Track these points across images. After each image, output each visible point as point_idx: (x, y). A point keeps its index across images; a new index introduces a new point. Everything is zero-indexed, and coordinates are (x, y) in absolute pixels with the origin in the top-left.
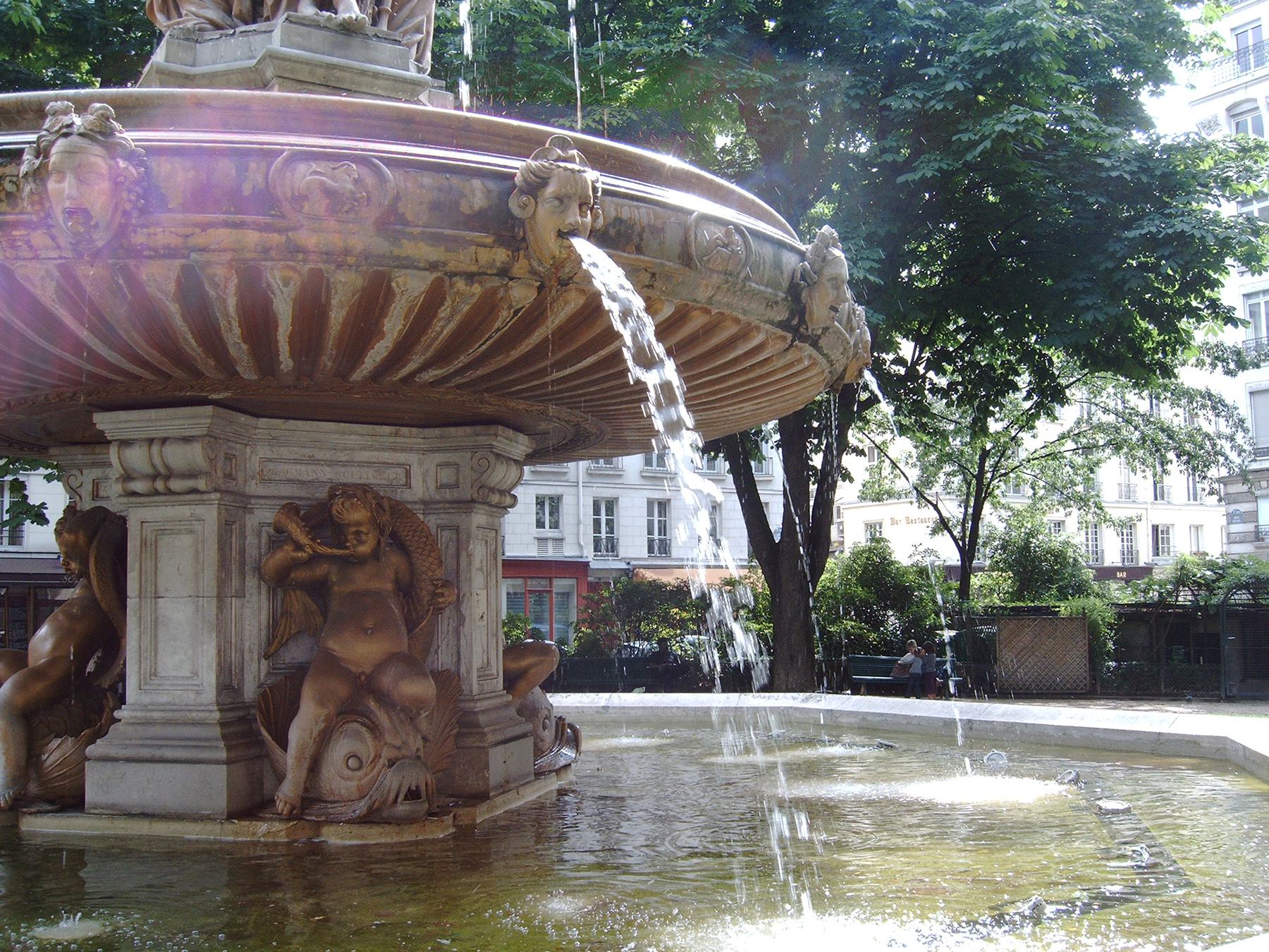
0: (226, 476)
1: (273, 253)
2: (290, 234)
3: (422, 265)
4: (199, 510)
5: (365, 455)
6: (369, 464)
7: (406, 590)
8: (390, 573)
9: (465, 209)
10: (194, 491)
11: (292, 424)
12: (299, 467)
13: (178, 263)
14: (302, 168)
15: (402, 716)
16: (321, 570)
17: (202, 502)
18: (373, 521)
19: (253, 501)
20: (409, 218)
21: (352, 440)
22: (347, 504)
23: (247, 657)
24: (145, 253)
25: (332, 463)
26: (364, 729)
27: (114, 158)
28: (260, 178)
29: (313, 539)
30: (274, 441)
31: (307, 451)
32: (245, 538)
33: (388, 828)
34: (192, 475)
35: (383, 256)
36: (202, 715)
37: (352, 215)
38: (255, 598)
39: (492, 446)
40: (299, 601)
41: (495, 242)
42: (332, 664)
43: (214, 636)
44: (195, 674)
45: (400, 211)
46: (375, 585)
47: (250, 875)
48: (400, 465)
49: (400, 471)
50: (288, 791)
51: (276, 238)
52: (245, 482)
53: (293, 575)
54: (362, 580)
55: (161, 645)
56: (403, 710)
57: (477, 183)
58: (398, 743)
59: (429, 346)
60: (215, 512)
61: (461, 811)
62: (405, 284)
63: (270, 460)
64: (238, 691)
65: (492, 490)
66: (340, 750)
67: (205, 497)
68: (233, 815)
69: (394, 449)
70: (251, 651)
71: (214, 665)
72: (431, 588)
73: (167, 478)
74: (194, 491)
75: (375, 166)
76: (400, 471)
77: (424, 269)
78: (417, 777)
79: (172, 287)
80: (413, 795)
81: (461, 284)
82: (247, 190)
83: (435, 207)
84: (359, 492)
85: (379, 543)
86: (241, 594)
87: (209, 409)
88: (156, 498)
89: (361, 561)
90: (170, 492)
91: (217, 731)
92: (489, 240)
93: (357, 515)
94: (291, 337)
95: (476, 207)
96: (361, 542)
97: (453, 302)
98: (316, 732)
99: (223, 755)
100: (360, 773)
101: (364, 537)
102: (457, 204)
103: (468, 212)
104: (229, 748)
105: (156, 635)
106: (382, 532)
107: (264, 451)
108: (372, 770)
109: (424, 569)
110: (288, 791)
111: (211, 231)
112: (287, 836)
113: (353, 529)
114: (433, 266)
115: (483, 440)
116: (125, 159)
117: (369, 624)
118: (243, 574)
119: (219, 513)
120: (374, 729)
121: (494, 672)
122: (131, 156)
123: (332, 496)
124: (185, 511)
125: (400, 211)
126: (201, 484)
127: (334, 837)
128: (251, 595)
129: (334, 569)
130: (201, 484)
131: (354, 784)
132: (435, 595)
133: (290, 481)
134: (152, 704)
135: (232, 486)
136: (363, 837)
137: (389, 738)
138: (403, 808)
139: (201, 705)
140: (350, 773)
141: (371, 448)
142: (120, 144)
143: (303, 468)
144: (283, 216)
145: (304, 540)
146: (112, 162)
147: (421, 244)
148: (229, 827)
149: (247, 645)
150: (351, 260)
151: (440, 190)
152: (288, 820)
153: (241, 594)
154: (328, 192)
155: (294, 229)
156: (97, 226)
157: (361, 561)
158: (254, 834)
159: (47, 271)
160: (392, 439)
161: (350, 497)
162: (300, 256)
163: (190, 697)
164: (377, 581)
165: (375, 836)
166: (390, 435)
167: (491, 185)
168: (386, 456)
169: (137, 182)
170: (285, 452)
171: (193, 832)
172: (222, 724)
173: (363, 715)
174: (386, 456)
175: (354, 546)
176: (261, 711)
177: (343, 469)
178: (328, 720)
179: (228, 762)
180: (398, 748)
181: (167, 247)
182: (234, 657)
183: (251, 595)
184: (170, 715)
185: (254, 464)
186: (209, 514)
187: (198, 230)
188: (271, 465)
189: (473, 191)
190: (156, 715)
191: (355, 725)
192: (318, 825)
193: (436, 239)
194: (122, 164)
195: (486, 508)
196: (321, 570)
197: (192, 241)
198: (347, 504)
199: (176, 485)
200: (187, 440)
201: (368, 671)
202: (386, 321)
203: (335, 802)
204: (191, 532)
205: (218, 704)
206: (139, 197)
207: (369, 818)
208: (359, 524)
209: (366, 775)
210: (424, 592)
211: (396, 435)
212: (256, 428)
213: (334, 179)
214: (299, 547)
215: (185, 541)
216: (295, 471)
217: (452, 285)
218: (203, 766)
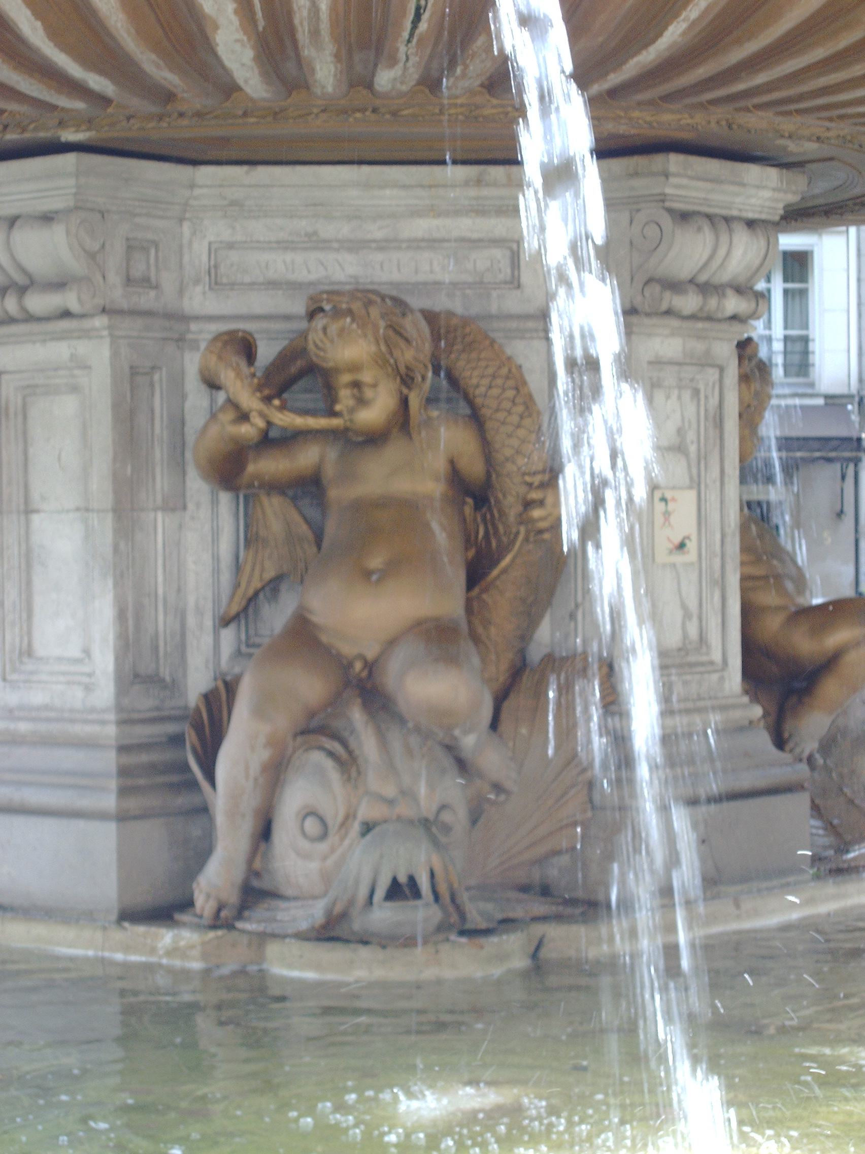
0: (129, 281)
4: (83, 348)
5: (422, 227)
6: (432, 243)
7: (474, 494)
8: (440, 464)
10: (66, 314)
11: (263, 173)
12: (289, 256)
15: (414, 740)
16: (307, 457)
17: (86, 334)
18: (381, 361)
19: (194, 327)
21: (390, 198)
22: (334, 328)
23: (191, 621)
25: (355, 246)
26: (329, 764)
29: (268, 400)
30: (235, 209)
31: (303, 225)
32: (184, 397)
33: (364, 952)
34: (59, 285)
36: (89, 729)
38: (205, 513)
39: (662, 198)
40: (275, 513)
42: (303, 636)
43: (110, 583)
44: (87, 652)
46: (403, 486)
47: (153, 1020)
48: (496, 242)
49: (500, 255)
50: (216, 879)
52: (181, 292)
53: (251, 468)
54: (380, 476)
55: (38, 600)
56: (418, 729)
58: (390, 791)
59: (315, 33)
60: (106, 353)
61: (554, 932)
63: (231, 246)
64: (173, 686)
65: (674, 286)
66: (296, 796)
67: (87, 324)
68: (131, 915)
69: (481, 211)
70: (199, 612)
71: (111, 637)
72: (522, 489)
73: (22, 290)
74: (66, 314)
76: (500, 255)
78: (415, 859)
80: (401, 890)
84: (357, 306)
85: (404, 402)
86: (176, 504)
87: (70, 159)
88: (65, 324)
89: (374, 439)
90: (30, 318)
91: (109, 760)
93: (349, 349)
94: (53, 34)
96: (362, 402)
98: (255, 768)
99: (109, 801)
100: (323, 847)
101: (368, 393)
104: (124, 792)
105: (29, 583)
106: (406, 379)
107: (217, 230)
108: (342, 839)
109: (508, 452)
110: (216, 879)
112: (204, 956)
113: (346, 378)
115: (642, 185)
117: (376, 562)
118: (178, 465)
119: (115, 354)
120: (348, 763)
121: (717, 656)
123: (313, 313)
124: (61, 351)
126: (70, 299)
127: (293, 966)
128: (198, 505)
129: (332, 454)
130: (70, 299)
131: (314, 866)
132: (528, 504)
133: (272, 285)
134: (21, 708)
135: (147, 300)
136: (318, 967)
137: (373, 781)
138: (384, 915)
139: (93, 710)
140: (305, 845)
141: (433, 211)
143: (299, 258)
145: (249, 400)
148: (117, 935)
149: (191, 600)
152: (214, 927)
153: (176, 504)
157: (374, 439)
158: (153, 951)
160: (472, 192)
161: (338, 313)
163: (76, 697)
164: (415, 473)
165: (354, 969)
166: (467, 184)
168: (466, 226)
170: (258, 229)
171: (74, 944)
172: (123, 749)
173: (335, 736)
174: (466, 226)
175: (352, 411)
176: (198, 727)
177: (379, 257)
178: (272, 742)
179: (122, 817)
180: (391, 802)
182: (161, 622)
183: (198, 505)
184: (42, 727)
185: (198, 255)
186: (95, 355)
188: (234, 256)
190: (23, 727)
191: (317, 757)
192: (263, 937)
195: (674, 323)
196: (307, 457)
198: (334, 328)
199: (37, 303)
200: (47, 218)
201: (370, 655)
203: (296, 898)
204: (75, 389)
205: (119, 708)
207: (332, 931)
208: (355, 368)
209: (333, 850)
210: (510, 499)
211: (479, 182)
212: (192, 186)
214: (243, 417)
215: (66, 407)
216: (280, 264)
218: (81, 824)
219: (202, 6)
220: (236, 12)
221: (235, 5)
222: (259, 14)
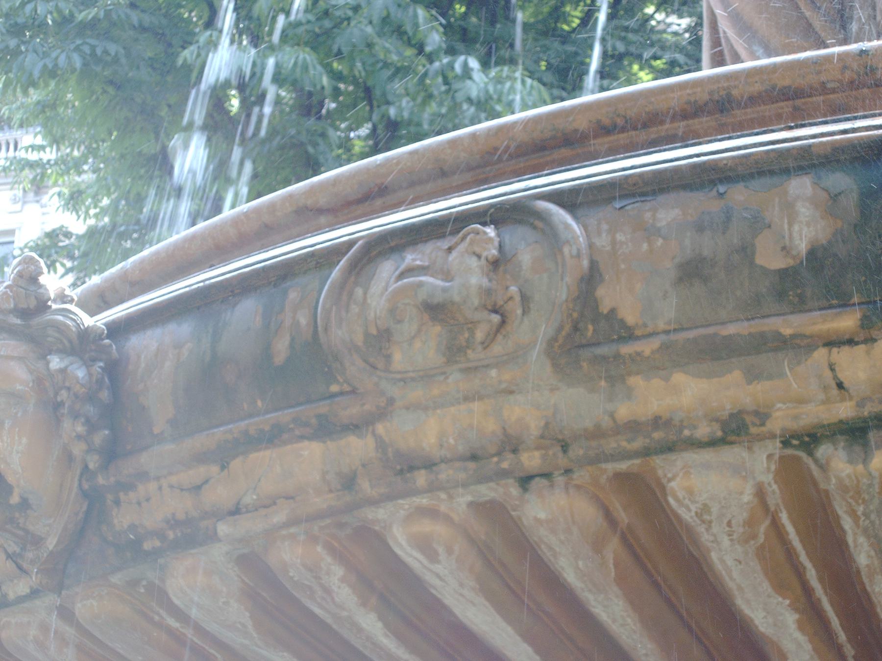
1: (365, 486)
2: (380, 428)
3: (703, 431)
9: (770, 259)
13: (218, 552)
14: (387, 269)
20: (630, 320)
24: (147, 546)
27: (43, 357)
28: (303, 320)
35: (597, 433)
37: (497, 348)
41: (866, 323)
45: (605, 308)
51: (358, 448)
57: (801, 187)
62: (690, 492)
75: (540, 215)
77: (713, 443)
79: (238, 612)
81: (838, 463)
82: (281, 347)
83: (692, 271)
92: (847, 322)
95: (802, 246)
97: (853, 513)
102: (746, 251)
103: (778, 263)
111: (236, 464)
114: (734, 430)
116: (62, 352)
122: (83, 344)
125: (605, 308)
142: (60, 328)
144: (354, 392)
146: (40, 365)
147: (679, 378)
150: (531, 460)
151: (700, 228)
154: (436, 310)
155: (382, 414)
156: (25, 504)
159: (44, 628)
162: (421, 478)
167: (841, 181)
169: (91, 398)
181: (174, 523)
187: (215, 469)
189: (789, 208)
193: (713, 353)
194: (56, 362)
197: (220, 494)
202: (739, 602)
206: (92, 427)
213: (447, 276)
217: (823, 468)
219: (752, 620)
220: (801, 627)
221: (797, 616)
222: (842, 637)
